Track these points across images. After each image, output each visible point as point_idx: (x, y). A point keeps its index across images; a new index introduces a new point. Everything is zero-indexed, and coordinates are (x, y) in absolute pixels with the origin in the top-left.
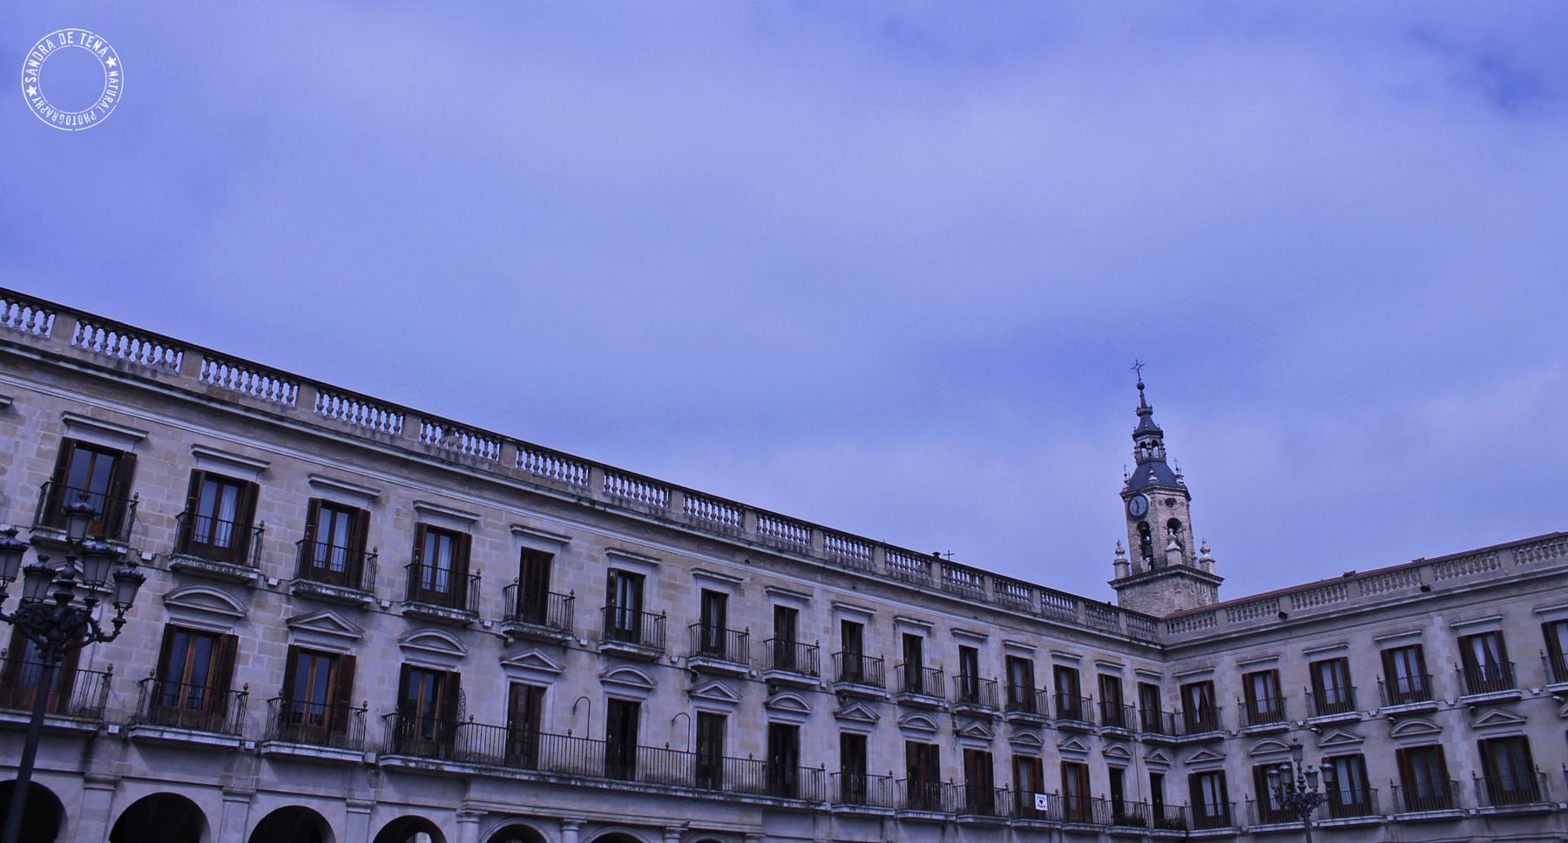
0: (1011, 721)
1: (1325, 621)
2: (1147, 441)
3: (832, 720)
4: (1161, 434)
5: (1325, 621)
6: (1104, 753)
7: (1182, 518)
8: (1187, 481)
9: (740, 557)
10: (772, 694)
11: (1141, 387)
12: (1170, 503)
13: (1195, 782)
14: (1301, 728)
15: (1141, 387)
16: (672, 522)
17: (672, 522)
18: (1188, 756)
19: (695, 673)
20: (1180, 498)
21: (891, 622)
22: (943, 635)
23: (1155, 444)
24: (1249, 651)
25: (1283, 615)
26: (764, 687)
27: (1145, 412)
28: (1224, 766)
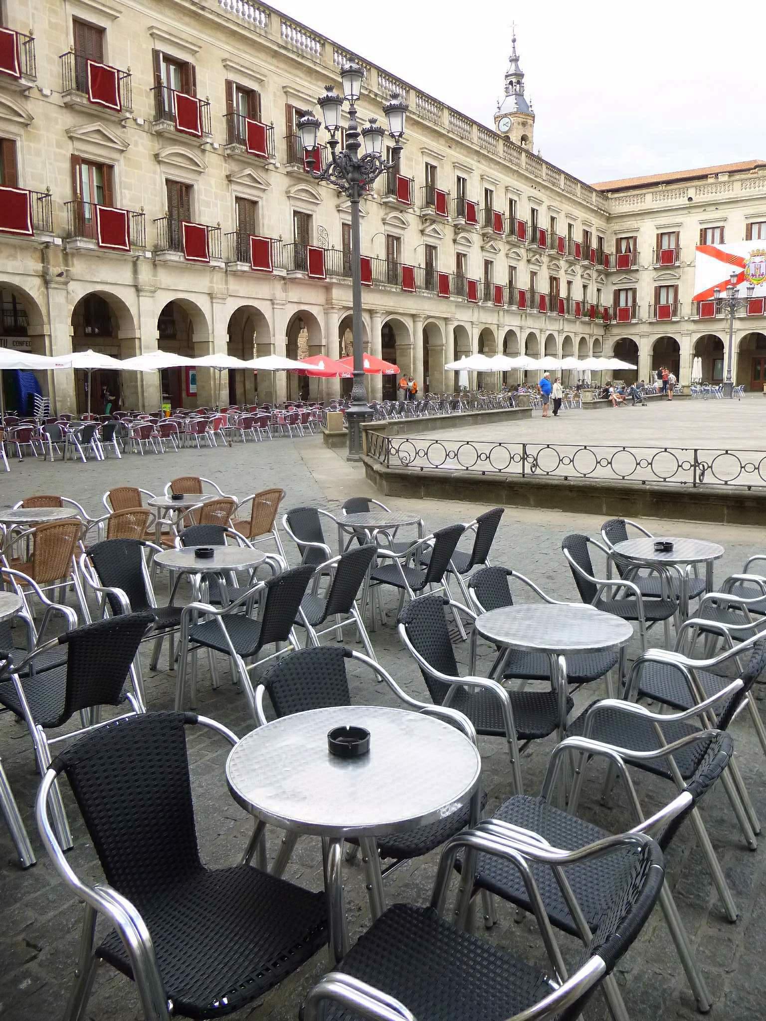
0: (549, 256)
1: (716, 204)
2: (514, 80)
3: (480, 250)
4: (522, 75)
5: (716, 204)
6: (582, 276)
7: (529, 135)
8: (536, 109)
9: (442, 141)
10: (456, 234)
11: (514, 41)
12: (524, 124)
13: (617, 293)
14: (689, 265)
15: (514, 41)
16: (414, 113)
17: (414, 113)
18: (615, 279)
19: (424, 219)
20: (530, 122)
21: (504, 190)
22: (524, 198)
23: (519, 82)
24: (663, 220)
25: (690, 199)
26: (452, 229)
27: (515, 60)
28: (636, 286)
